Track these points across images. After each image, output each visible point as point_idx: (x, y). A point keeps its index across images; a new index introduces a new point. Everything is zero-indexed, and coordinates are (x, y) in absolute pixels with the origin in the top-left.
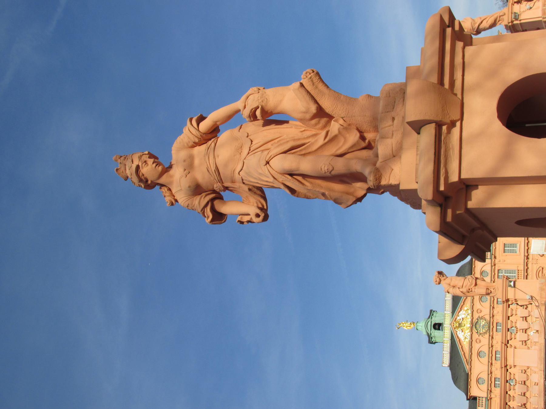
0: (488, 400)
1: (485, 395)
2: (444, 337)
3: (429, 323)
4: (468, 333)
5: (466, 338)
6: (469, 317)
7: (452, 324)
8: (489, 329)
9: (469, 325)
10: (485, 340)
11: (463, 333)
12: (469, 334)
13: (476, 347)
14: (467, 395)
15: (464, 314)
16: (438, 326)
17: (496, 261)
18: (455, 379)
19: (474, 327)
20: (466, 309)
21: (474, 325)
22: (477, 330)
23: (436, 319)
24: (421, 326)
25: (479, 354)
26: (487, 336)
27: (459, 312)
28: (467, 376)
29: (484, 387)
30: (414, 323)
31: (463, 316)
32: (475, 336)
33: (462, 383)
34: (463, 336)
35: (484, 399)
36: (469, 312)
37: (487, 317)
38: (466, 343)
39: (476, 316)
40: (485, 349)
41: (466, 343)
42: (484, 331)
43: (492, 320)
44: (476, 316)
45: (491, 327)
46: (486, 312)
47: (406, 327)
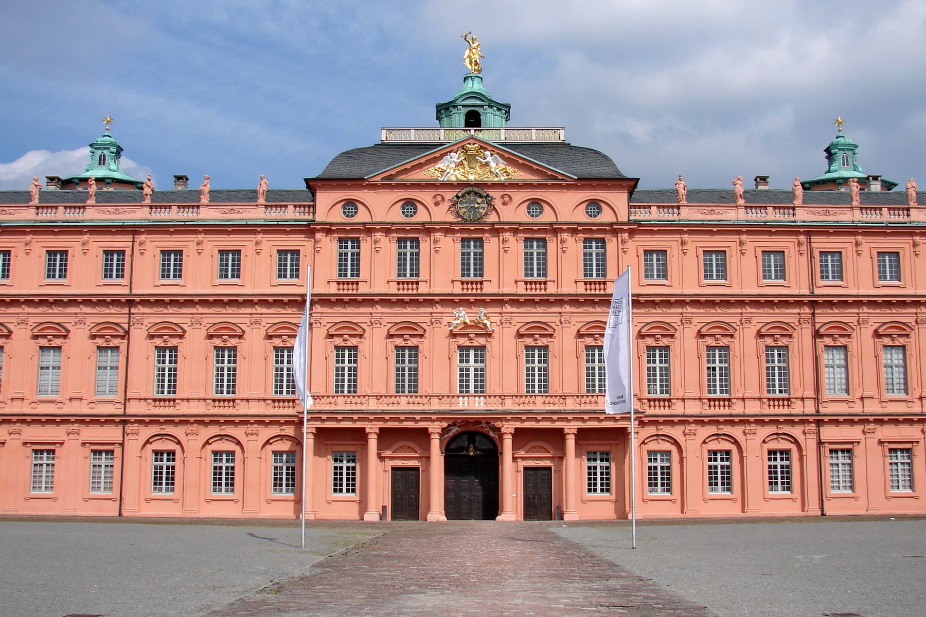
0: (308, 225)
1: (320, 218)
4: (455, 175)
5: (443, 172)
7: (471, 141)
8: (466, 222)
9: (472, 178)
10: (442, 214)
11: (453, 165)
12: (453, 178)
13: (426, 196)
15: (496, 168)
17: (626, 236)
19: (470, 189)
20: (510, 169)
22: (463, 196)
26: (451, 218)
27: (502, 156)
28: (357, 182)
29: (337, 216)
31: (493, 165)
32: (449, 195)
35: (311, 217)
37: (492, 218)
38: (430, 173)
39: (495, 194)
40: (421, 216)
41: (430, 173)
42: (461, 212)
44: (495, 194)
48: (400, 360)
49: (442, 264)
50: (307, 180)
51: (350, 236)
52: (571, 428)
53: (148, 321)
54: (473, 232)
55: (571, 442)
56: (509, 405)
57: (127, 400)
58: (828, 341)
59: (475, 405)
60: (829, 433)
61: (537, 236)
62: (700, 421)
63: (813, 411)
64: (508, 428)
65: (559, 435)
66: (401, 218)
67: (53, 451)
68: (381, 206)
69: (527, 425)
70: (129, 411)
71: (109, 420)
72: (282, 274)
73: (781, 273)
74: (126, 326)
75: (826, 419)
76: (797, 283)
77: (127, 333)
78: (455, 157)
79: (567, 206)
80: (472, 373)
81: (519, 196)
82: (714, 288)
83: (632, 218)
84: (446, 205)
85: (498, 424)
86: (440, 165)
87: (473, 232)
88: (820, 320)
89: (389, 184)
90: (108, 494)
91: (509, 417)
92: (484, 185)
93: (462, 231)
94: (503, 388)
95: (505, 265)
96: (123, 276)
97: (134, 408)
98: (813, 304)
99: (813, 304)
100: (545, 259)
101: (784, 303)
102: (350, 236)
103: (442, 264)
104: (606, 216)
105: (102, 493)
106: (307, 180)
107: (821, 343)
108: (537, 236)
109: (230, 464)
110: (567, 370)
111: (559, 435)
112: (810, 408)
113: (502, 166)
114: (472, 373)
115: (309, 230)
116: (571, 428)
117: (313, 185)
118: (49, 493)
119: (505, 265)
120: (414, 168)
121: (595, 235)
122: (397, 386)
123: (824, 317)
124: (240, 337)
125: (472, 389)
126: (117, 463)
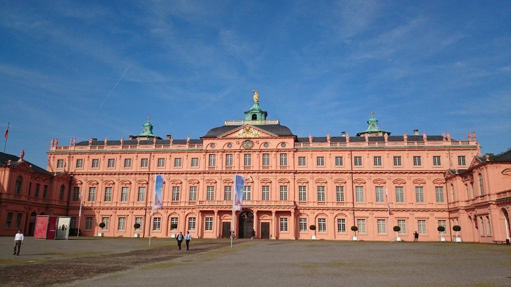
2: (248, 121)
3: (256, 112)
4: (244, 136)
6: (253, 136)
9: (248, 136)
13: (234, 142)
14: (203, 137)
15: (254, 133)
16: (254, 117)
18: (213, 130)
21: (248, 140)
23: (259, 116)
24: (256, 106)
25: (229, 144)
26: (242, 148)
28: (214, 137)
29: (209, 148)
30: (258, 101)
32: (241, 141)
33: (213, 134)
34: (241, 133)
36: (257, 136)
37: (254, 148)
41: (236, 135)
43: (252, 151)
44: (254, 141)
45: (248, 151)
46: (256, 147)
47: (255, 97)
49: (237, 162)
50: (200, 138)
51: (211, 153)
54: (247, 151)
56: (255, 203)
58: (357, 185)
59: (246, 203)
60: (357, 214)
61: (265, 153)
62: (314, 209)
63: (352, 207)
64: (255, 210)
66: (228, 148)
68: (220, 144)
69: (261, 210)
73: (341, 164)
74: (147, 181)
75: (356, 209)
76: (347, 165)
78: (241, 131)
79: (274, 143)
80: (247, 194)
81: (261, 141)
82: (320, 168)
83: (295, 147)
84: (240, 144)
85: (252, 209)
86: (239, 132)
87: (247, 151)
88: (354, 178)
89: (224, 138)
91: (255, 207)
92: (251, 138)
93: (244, 152)
94: (255, 199)
95: (256, 162)
98: (352, 173)
99: (352, 173)
100: (281, 161)
102: (211, 153)
103: (237, 162)
104: (287, 147)
106: (200, 138)
107: (355, 185)
108: (265, 153)
109: (194, 221)
110: (275, 192)
112: (350, 206)
113: (256, 133)
114: (247, 194)
115: (201, 151)
116: (274, 210)
117: (203, 138)
119: (256, 162)
120: (230, 134)
121: (282, 152)
123: (356, 177)
125: (247, 199)
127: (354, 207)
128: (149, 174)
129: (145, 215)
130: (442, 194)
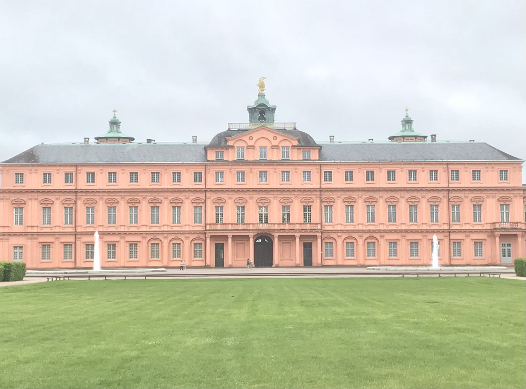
48: (131, 211)
52: (230, 235)
53: (83, 198)
55: (230, 240)
57: (76, 226)
65: (226, 237)
67: (50, 245)
70: (78, 231)
71: (70, 234)
72: (110, 181)
77: (76, 202)
90: (70, 260)
96: (72, 182)
97: (79, 230)
101: (310, 190)
105: (68, 260)
111: (226, 237)
116: (230, 235)
118: (48, 260)
122: (260, 220)
124: (160, 203)
126: (73, 249)
127: (321, 229)
128: (76, 192)
129: (75, 242)
130: (201, 214)
